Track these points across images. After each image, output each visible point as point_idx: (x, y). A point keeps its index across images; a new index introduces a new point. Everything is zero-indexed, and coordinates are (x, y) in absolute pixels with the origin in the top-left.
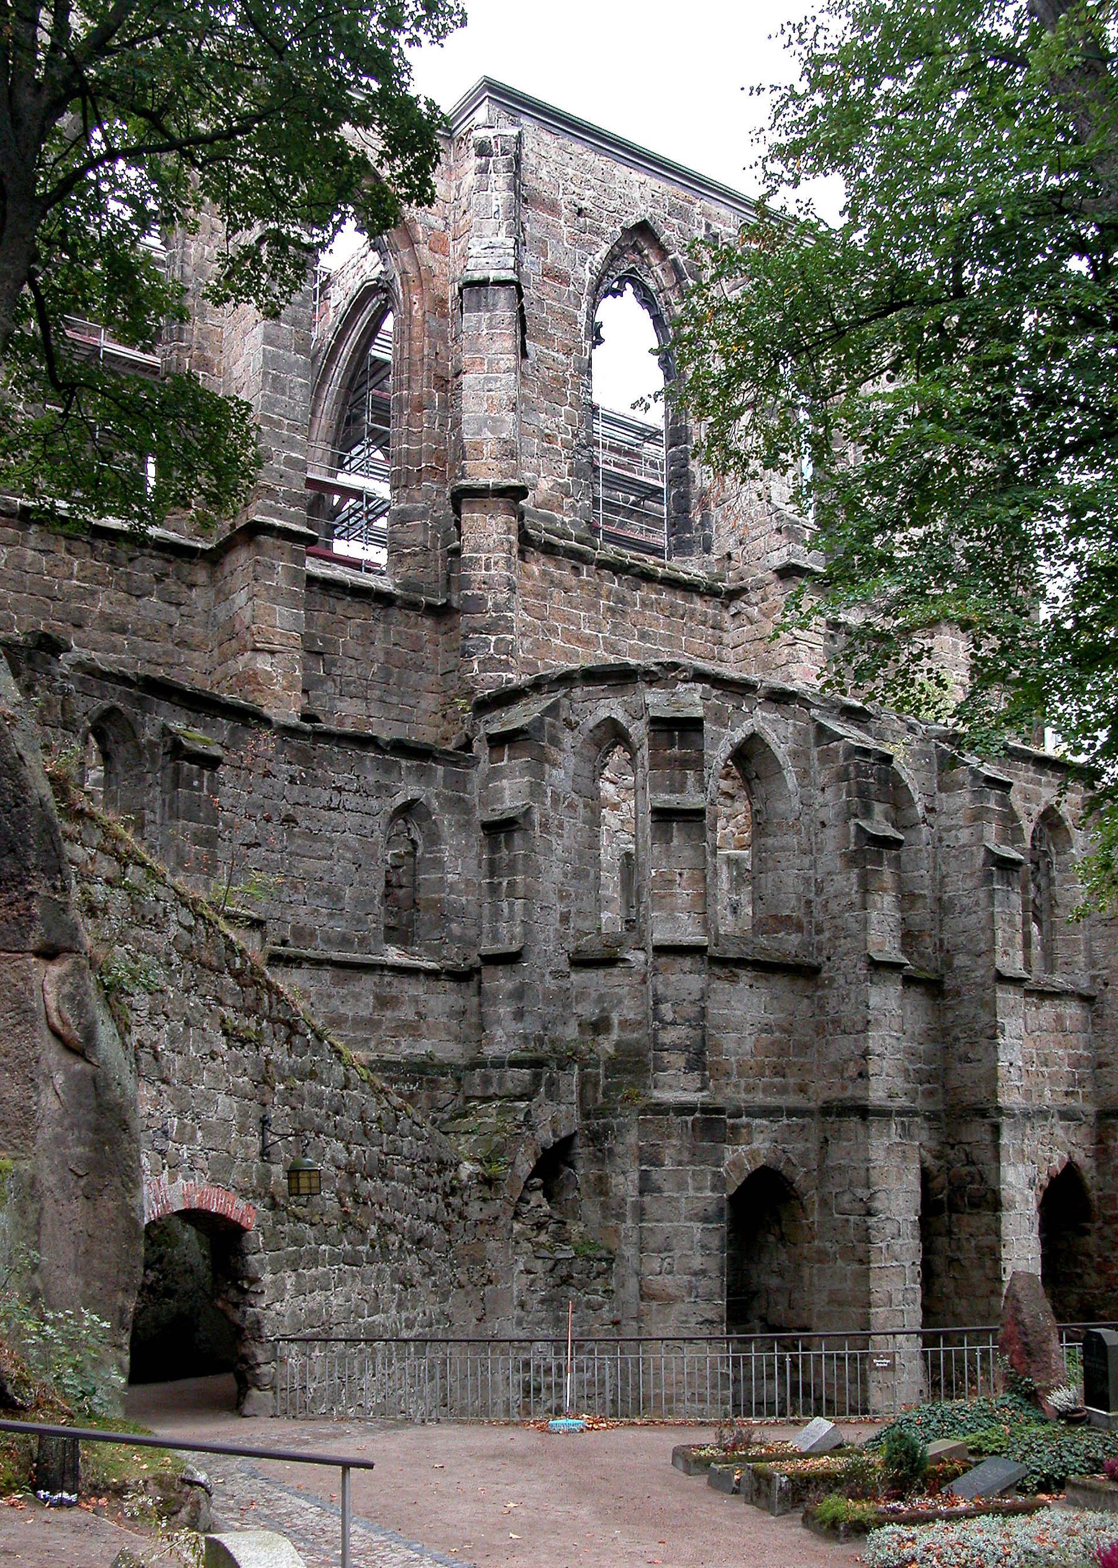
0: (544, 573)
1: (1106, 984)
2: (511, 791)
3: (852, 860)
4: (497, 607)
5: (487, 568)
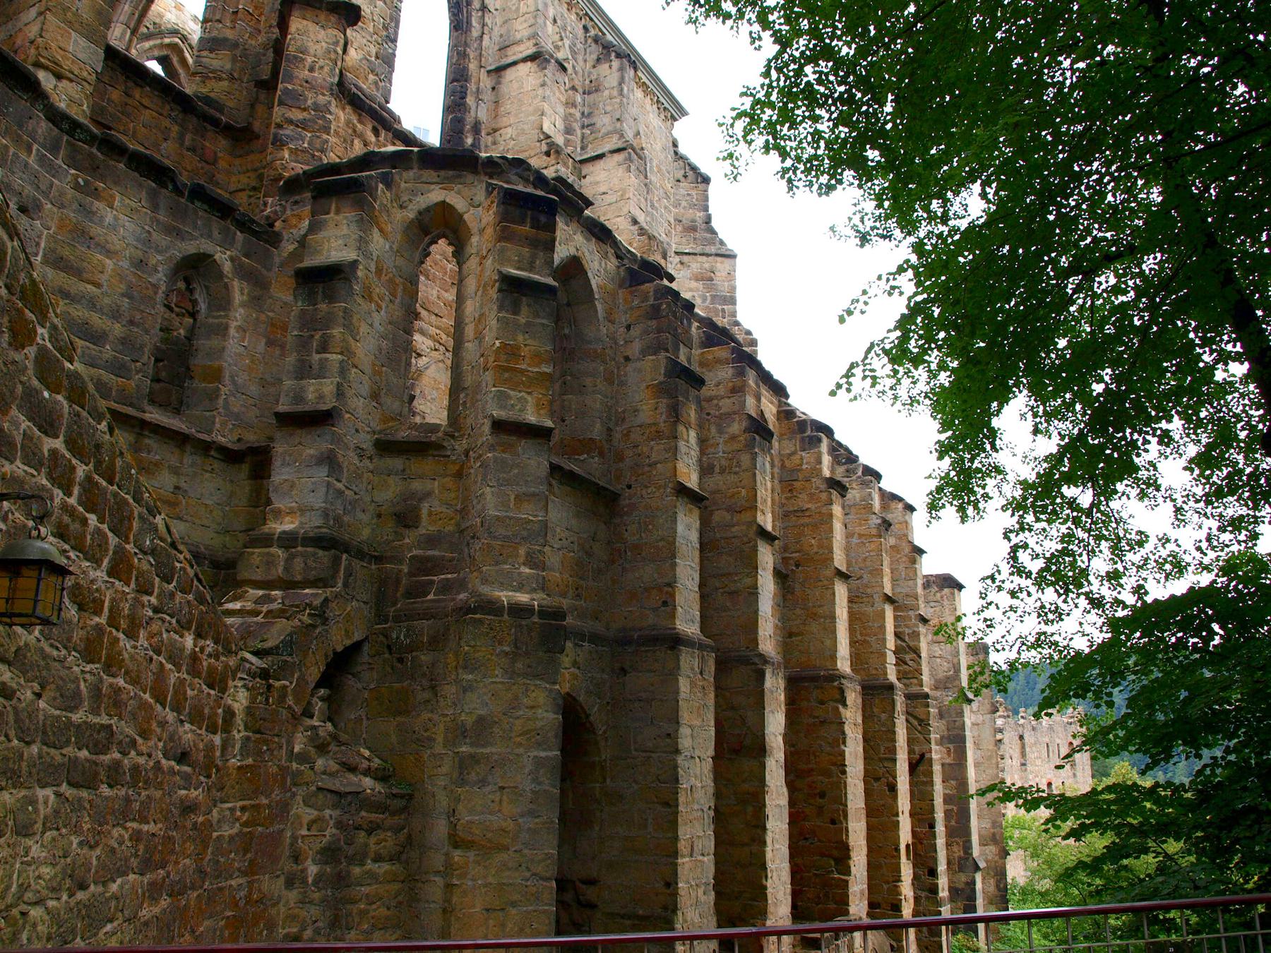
0: (348, 123)
1: (797, 566)
2: (337, 241)
3: (662, 390)
4: (316, 107)
5: (311, 70)
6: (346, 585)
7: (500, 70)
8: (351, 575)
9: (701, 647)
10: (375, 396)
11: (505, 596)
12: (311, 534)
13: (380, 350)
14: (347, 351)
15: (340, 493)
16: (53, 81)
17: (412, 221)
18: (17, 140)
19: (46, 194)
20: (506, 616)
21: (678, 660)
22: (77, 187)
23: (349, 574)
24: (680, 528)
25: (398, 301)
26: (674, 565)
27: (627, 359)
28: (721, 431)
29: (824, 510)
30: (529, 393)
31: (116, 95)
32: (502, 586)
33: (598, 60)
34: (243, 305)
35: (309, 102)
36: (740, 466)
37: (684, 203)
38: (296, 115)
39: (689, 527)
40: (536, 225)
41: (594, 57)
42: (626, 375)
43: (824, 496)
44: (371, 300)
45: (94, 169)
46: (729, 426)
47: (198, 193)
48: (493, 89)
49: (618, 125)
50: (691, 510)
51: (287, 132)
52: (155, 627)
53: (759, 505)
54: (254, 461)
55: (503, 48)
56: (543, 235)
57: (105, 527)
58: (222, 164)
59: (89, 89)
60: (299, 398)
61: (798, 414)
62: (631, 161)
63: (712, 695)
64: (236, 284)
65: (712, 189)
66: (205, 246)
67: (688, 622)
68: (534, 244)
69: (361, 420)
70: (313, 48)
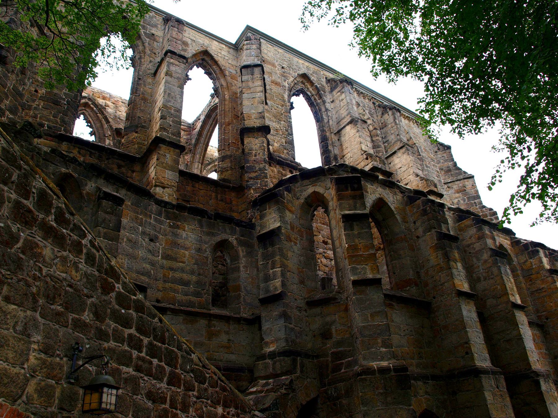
0: (279, 172)
1: (547, 319)
2: (272, 221)
3: (437, 247)
4: (260, 169)
5: (255, 156)
6: (302, 371)
7: (339, 132)
8: (304, 366)
9: (494, 373)
10: (302, 282)
11: (375, 364)
12: (281, 351)
13: (300, 262)
14: (283, 266)
15: (292, 329)
16: (162, 190)
17: (303, 203)
18: (146, 215)
19: (159, 232)
20: (377, 374)
21: (481, 383)
22: (170, 226)
23: (302, 366)
24: (465, 313)
25: (304, 239)
26: (466, 332)
27: (418, 237)
28: (478, 260)
29: (552, 286)
30: (366, 265)
31: (189, 188)
32: (374, 360)
33: (383, 114)
34: (244, 257)
35: (257, 168)
36: (493, 275)
37: (442, 161)
38: (253, 175)
39: (469, 311)
40: (353, 189)
41: (381, 113)
42: (419, 245)
43: (550, 279)
44: (291, 241)
45: (175, 218)
46: (482, 256)
47: (218, 216)
48: (338, 140)
49: (398, 137)
50: (468, 303)
51: (251, 183)
52: (198, 406)
53: (509, 292)
54: (255, 322)
55: (338, 123)
56: (358, 193)
57: (163, 364)
58: (234, 203)
59: (175, 189)
60: (267, 291)
61: (522, 241)
62: (408, 150)
63: (508, 399)
64: (240, 248)
65: (453, 151)
66: (224, 236)
67: (482, 360)
68: (354, 197)
69: (297, 295)
70: (254, 147)
